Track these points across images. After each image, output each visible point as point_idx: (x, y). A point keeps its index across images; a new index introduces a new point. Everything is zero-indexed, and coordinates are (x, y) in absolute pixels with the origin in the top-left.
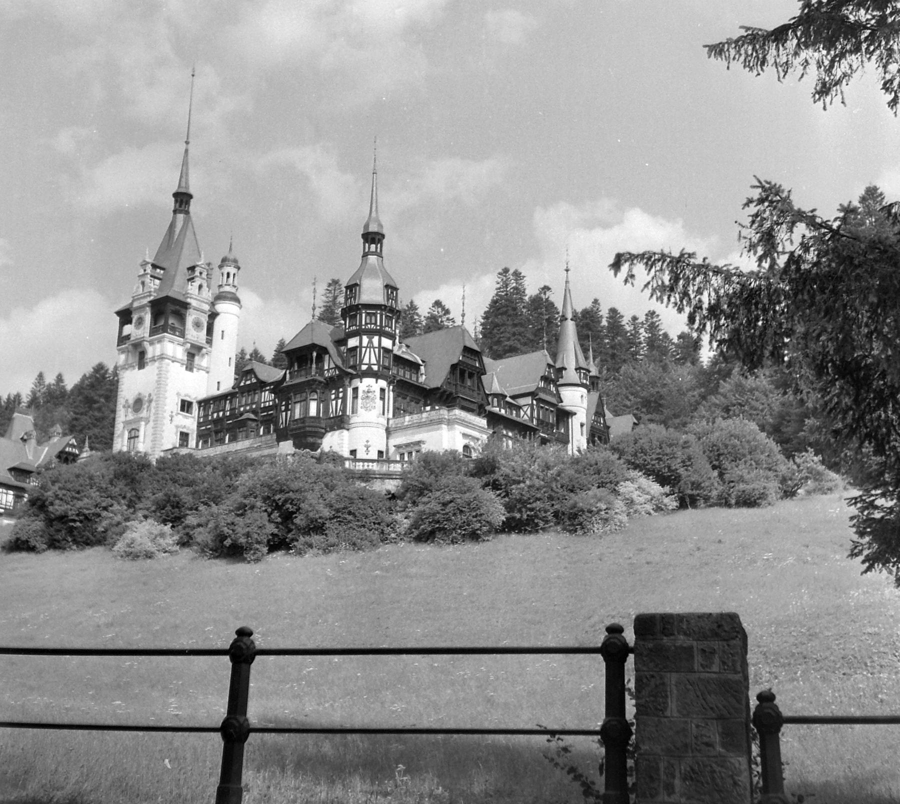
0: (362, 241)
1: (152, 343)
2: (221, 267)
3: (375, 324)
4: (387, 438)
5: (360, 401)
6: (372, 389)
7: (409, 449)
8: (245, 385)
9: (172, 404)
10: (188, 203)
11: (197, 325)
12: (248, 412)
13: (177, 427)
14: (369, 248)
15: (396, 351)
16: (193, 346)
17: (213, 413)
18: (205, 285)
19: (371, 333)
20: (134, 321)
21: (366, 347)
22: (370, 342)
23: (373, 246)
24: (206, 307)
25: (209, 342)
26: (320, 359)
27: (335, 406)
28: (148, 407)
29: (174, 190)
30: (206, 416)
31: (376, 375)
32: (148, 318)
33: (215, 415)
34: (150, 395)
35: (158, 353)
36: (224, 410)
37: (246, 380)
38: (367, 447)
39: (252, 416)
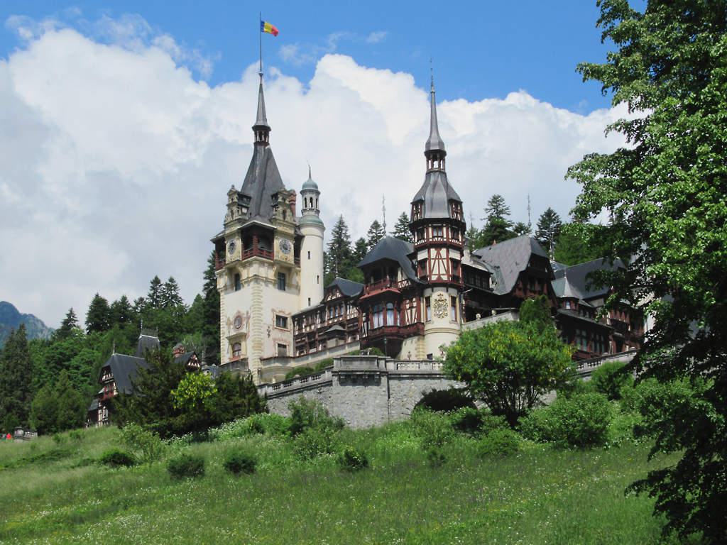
0: (425, 158)
1: (244, 266)
2: (303, 192)
3: (442, 237)
8: (331, 301)
9: (270, 320)
10: (266, 135)
11: (285, 248)
12: (336, 324)
13: (274, 340)
14: (433, 165)
15: (466, 260)
16: (282, 267)
17: (306, 327)
18: (288, 211)
19: (438, 246)
21: (435, 259)
22: (438, 254)
23: (436, 163)
25: (297, 261)
26: (394, 275)
29: (253, 125)
30: (300, 329)
31: (445, 285)
32: (239, 243)
33: (308, 329)
34: (247, 313)
35: (251, 275)
39: (339, 328)
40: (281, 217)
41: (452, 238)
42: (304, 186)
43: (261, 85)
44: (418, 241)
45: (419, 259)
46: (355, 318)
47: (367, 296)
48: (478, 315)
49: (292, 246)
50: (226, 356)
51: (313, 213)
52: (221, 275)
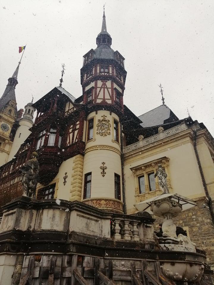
3: (108, 73)
4: (123, 165)
5: (95, 127)
6: (107, 119)
7: (149, 170)
19: (104, 79)
22: (104, 84)
24: (13, 121)
25: (12, 137)
27: (72, 137)
38: (103, 169)
40: (7, 112)
41: (117, 76)
42: (28, 104)
43: (18, 66)
44: (86, 79)
49: (10, 129)
51: (28, 116)
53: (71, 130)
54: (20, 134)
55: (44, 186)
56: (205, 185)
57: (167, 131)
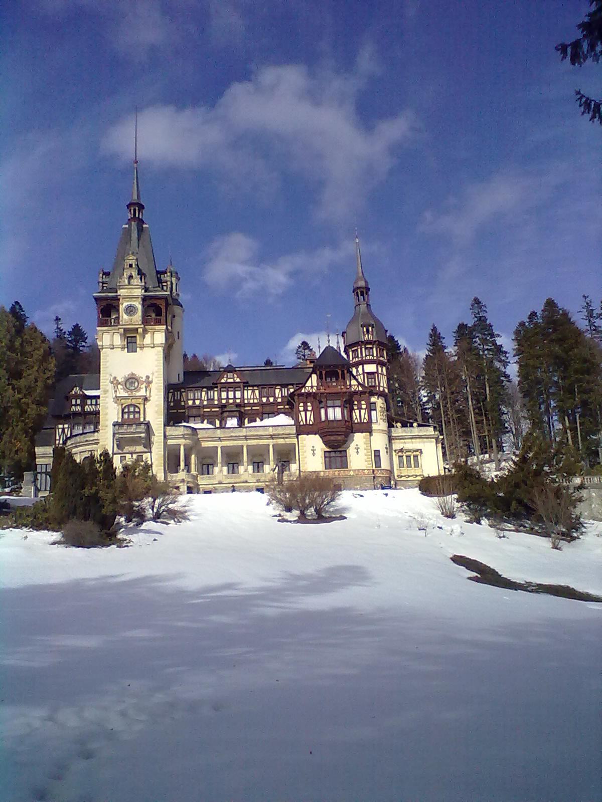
7: (408, 454)
20: (122, 308)
22: (382, 371)
28: (146, 387)
32: (140, 307)
34: (148, 377)
36: (201, 399)
37: (228, 378)
44: (366, 356)
45: (366, 371)
46: (254, 403)
47: (322, 391)
48: (399, 425)
50: (110, 413)
52: (107, 332)
53: (356, 407)
54: (178, 332)
55: (332, 450)
56: (439, 470)
57: (421, 428)
